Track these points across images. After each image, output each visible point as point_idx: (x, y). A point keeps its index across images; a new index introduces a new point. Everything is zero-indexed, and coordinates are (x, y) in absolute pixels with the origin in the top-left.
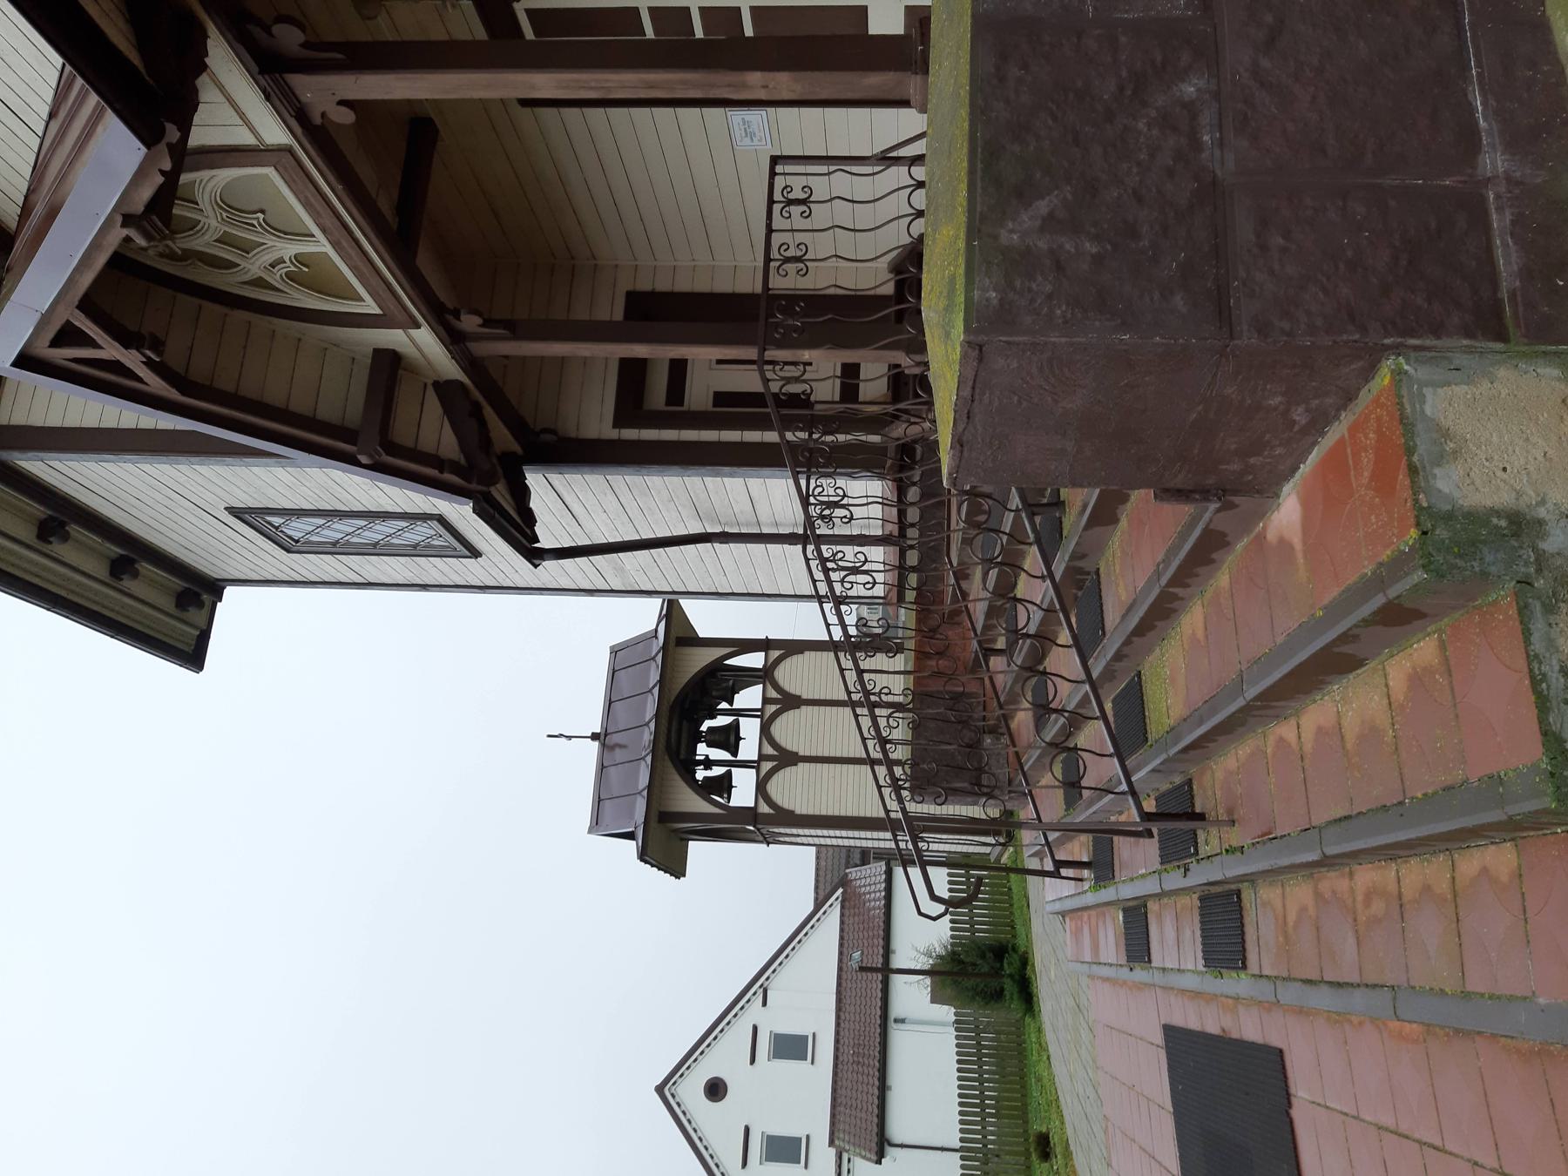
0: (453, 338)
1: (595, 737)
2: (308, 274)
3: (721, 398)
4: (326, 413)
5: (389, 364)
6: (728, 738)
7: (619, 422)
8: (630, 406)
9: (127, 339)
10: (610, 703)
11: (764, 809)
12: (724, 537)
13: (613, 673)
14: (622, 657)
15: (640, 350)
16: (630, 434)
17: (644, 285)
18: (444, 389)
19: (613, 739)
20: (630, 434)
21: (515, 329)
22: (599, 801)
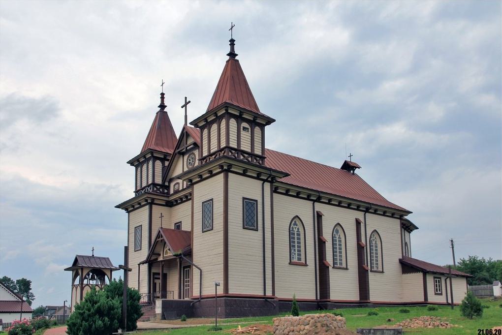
0: (162, 261)
1: (93, 255)
2: (167, 253)
3: (156, 283)
4: (155, 250)
5: (160, 255)
6: (93, 278)
7: (153, 273)
8: (154, 274)
9: (162, 240)
10: (99, 258)
11: (84, 285)
12: (139, 283)
13: (104, 258)
14: (107, 260)
15: (161, 275)
16: (152, 274)
17: (168, 275)
18: (157, 259)
19: (92, 260)
20: (152, 274)
21: (163, 267)
22: (83, 257)
